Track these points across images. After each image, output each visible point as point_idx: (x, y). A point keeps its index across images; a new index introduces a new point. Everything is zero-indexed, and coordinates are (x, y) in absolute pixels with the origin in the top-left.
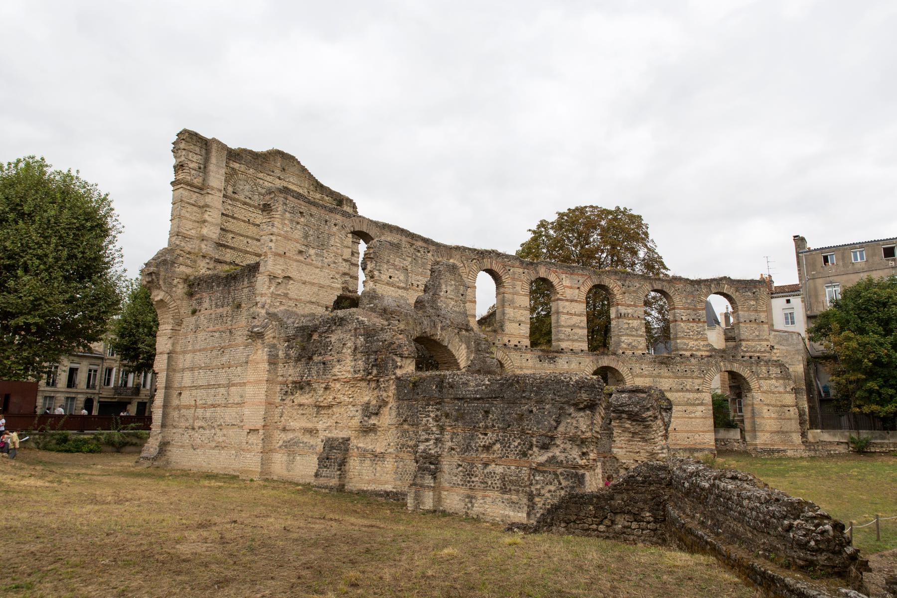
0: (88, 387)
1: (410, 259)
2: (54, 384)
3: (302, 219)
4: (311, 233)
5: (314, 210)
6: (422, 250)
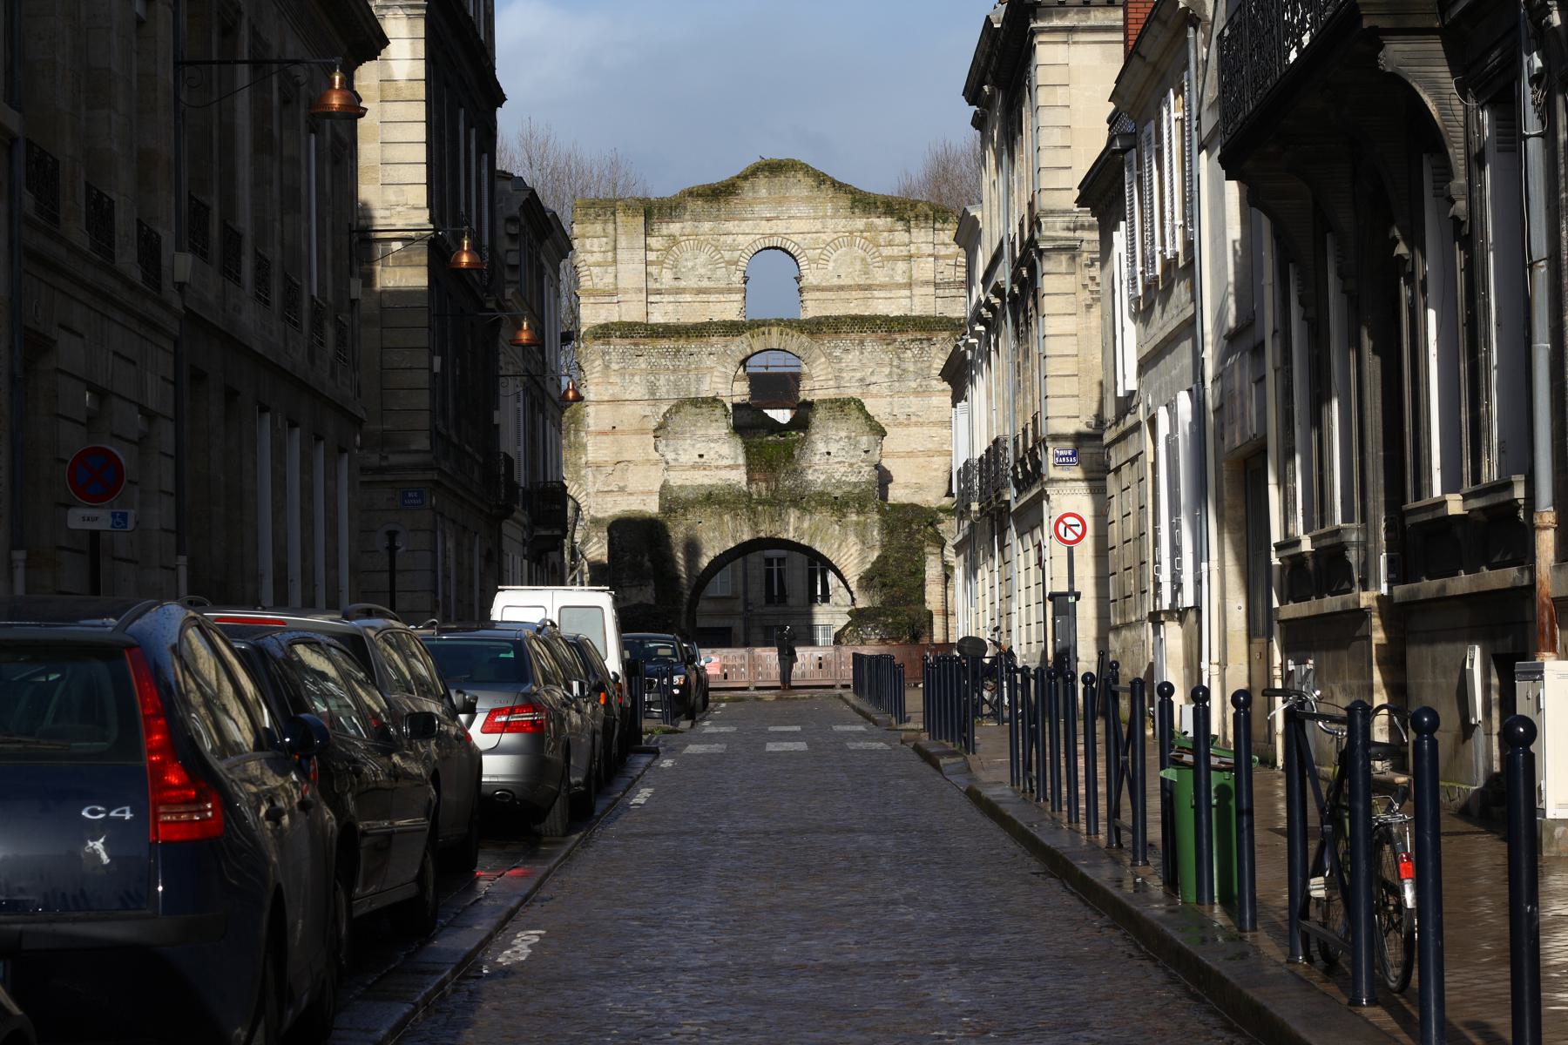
2: (783, 597)
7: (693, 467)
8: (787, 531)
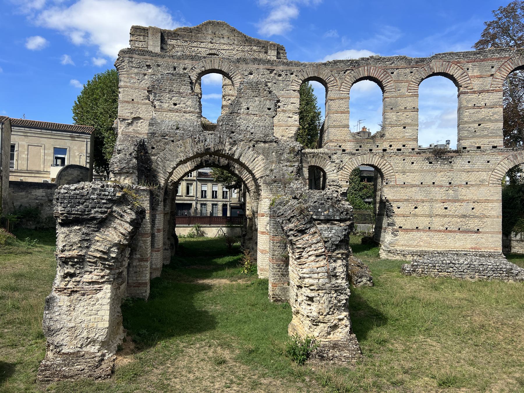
0: (213, 197)
2: (205, 197)
3: (150, 71)
6: (283, 74)
7: (170, 111)
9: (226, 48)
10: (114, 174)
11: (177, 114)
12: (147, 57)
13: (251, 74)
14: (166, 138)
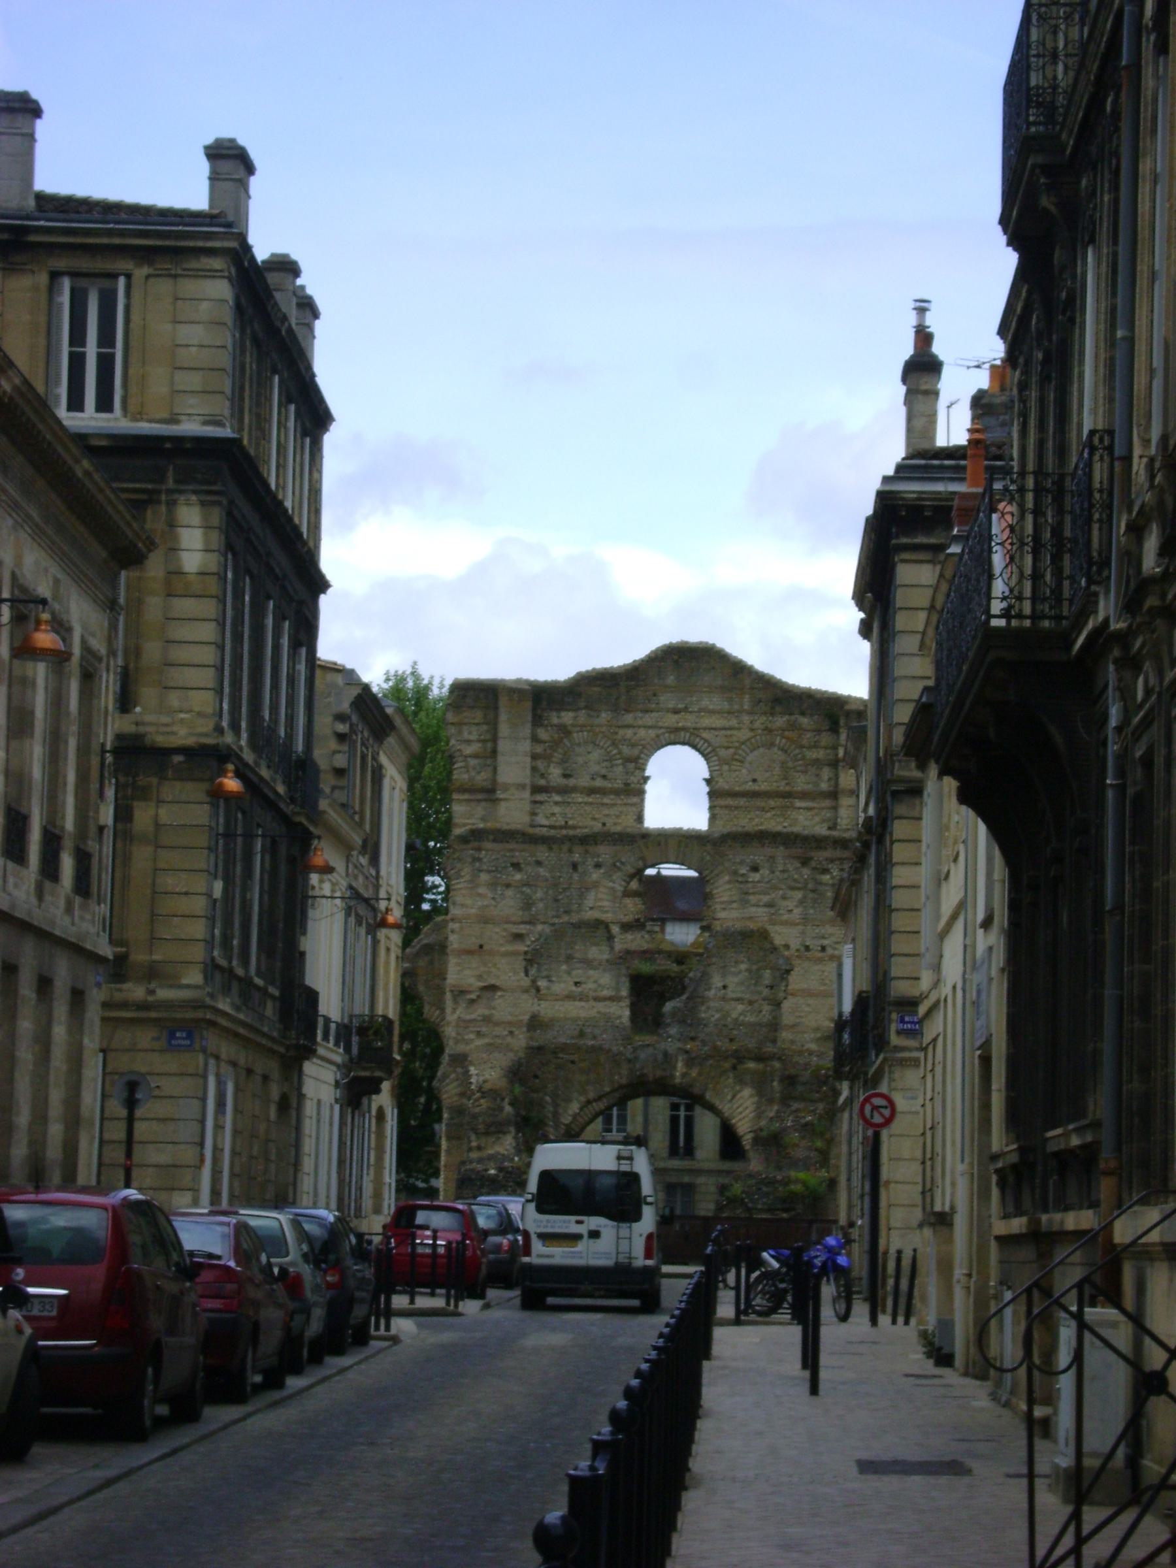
1: (799, 895)
2: (689, 1151)
3: (518, 877)
4: (539, 894)
5: (542, 853)
7: (570, 997)
8: (672, 1077)
9: (718, 722)
10: (476, 1134)
11: (583, 1004)
12: (512, 846)
13: (755, 869)
14: (561, 1055)
